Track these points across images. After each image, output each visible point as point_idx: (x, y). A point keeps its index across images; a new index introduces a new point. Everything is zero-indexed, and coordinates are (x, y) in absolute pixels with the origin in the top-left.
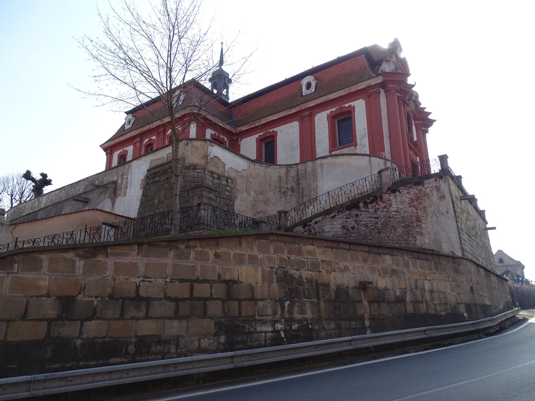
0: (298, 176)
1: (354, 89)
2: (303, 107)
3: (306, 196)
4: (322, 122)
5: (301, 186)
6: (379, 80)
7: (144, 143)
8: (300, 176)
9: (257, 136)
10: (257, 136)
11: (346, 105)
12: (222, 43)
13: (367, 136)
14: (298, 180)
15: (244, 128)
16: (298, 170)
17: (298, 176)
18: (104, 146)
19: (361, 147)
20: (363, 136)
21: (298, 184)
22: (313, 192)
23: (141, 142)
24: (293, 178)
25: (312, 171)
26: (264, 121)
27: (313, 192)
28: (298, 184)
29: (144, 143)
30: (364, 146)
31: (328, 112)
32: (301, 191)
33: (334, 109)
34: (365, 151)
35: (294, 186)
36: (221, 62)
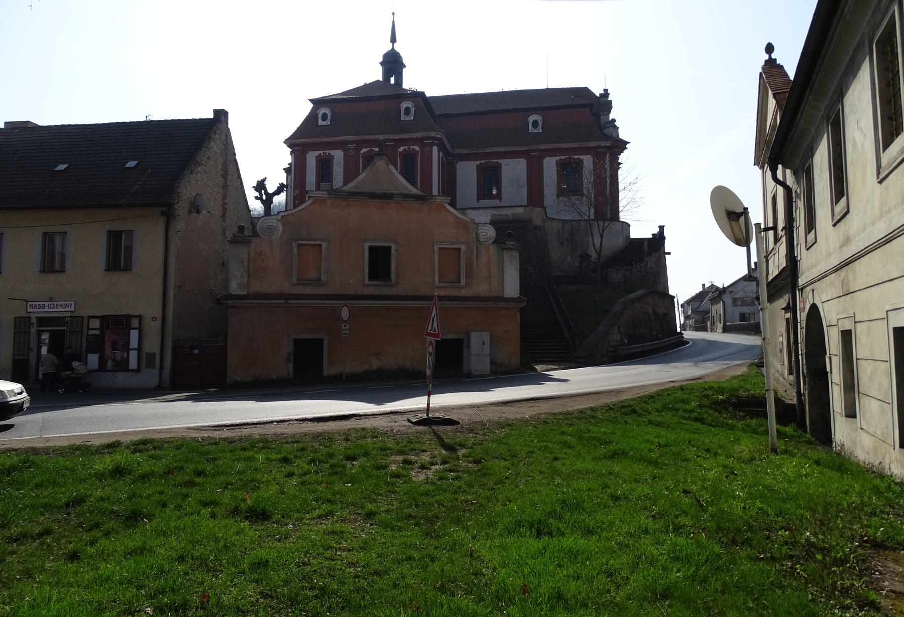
1: (585, 145)
2: (534, 147)
4: (550, 165)
6: (608, 144)
7: (362, 152)
9: (478, 162)
10: (478, 162)
11: (576, 157)
12: (393, 14)
15: (464, 152)
18: (293, 141)
23: (357, 150)
26: (488, 151)
29: (362, 152)
31: (558, 158)
33: (563, 157)
36: (393, 40)
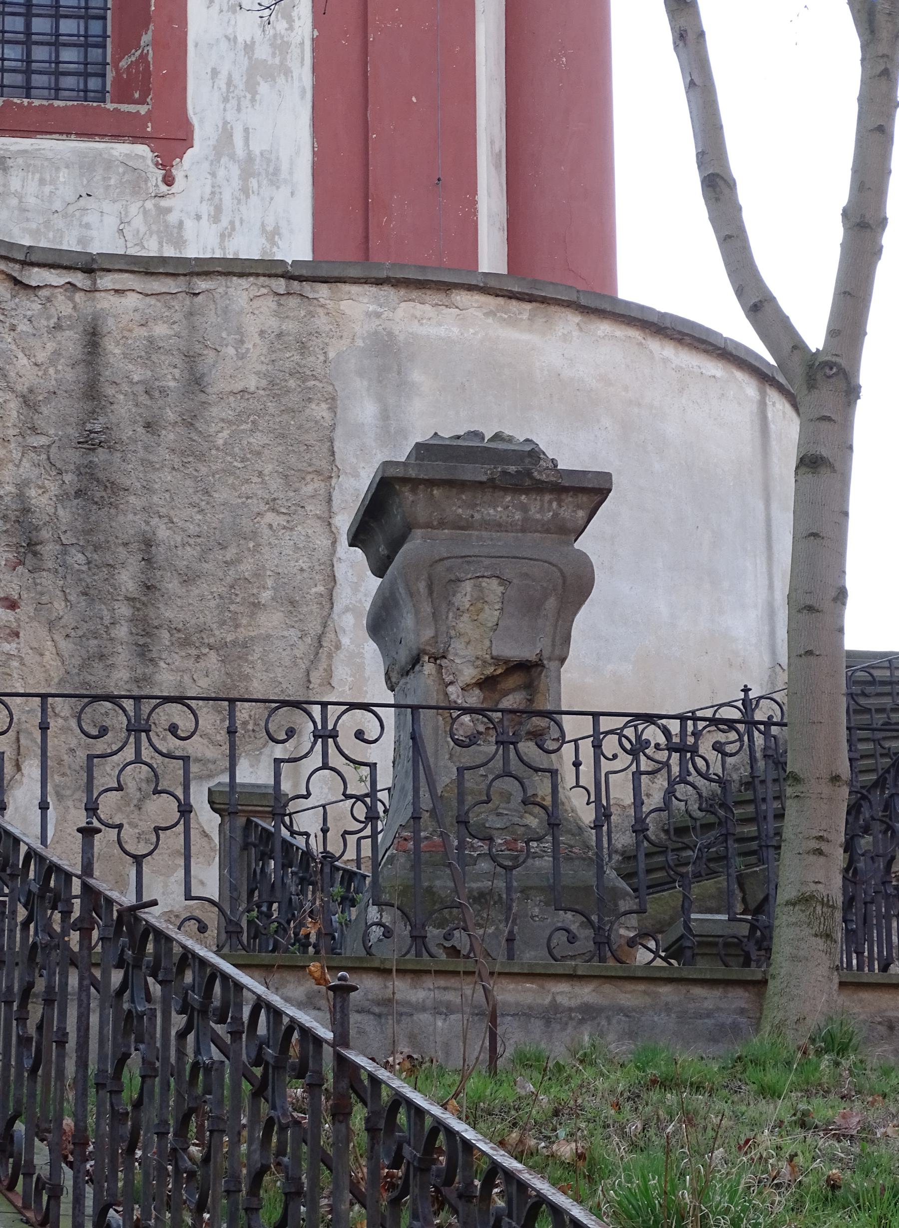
0: (92, 393)
3: (185, 640)
5: (128, 522)
8: (123, 411)
13: (303, 75)
14: (90, 442)
16: (93, 338)
17: (92, 393)
19: (230, 173)
20: (257, 72)
21: (93, 489)
22: (271, 621)
24: (28, 402)
25: (274, 387)
27: (271, 621)
28: (93, 489)
30: (258, 171)
32: (128, 580)
34: (272, 235)
35: (41, 500)
